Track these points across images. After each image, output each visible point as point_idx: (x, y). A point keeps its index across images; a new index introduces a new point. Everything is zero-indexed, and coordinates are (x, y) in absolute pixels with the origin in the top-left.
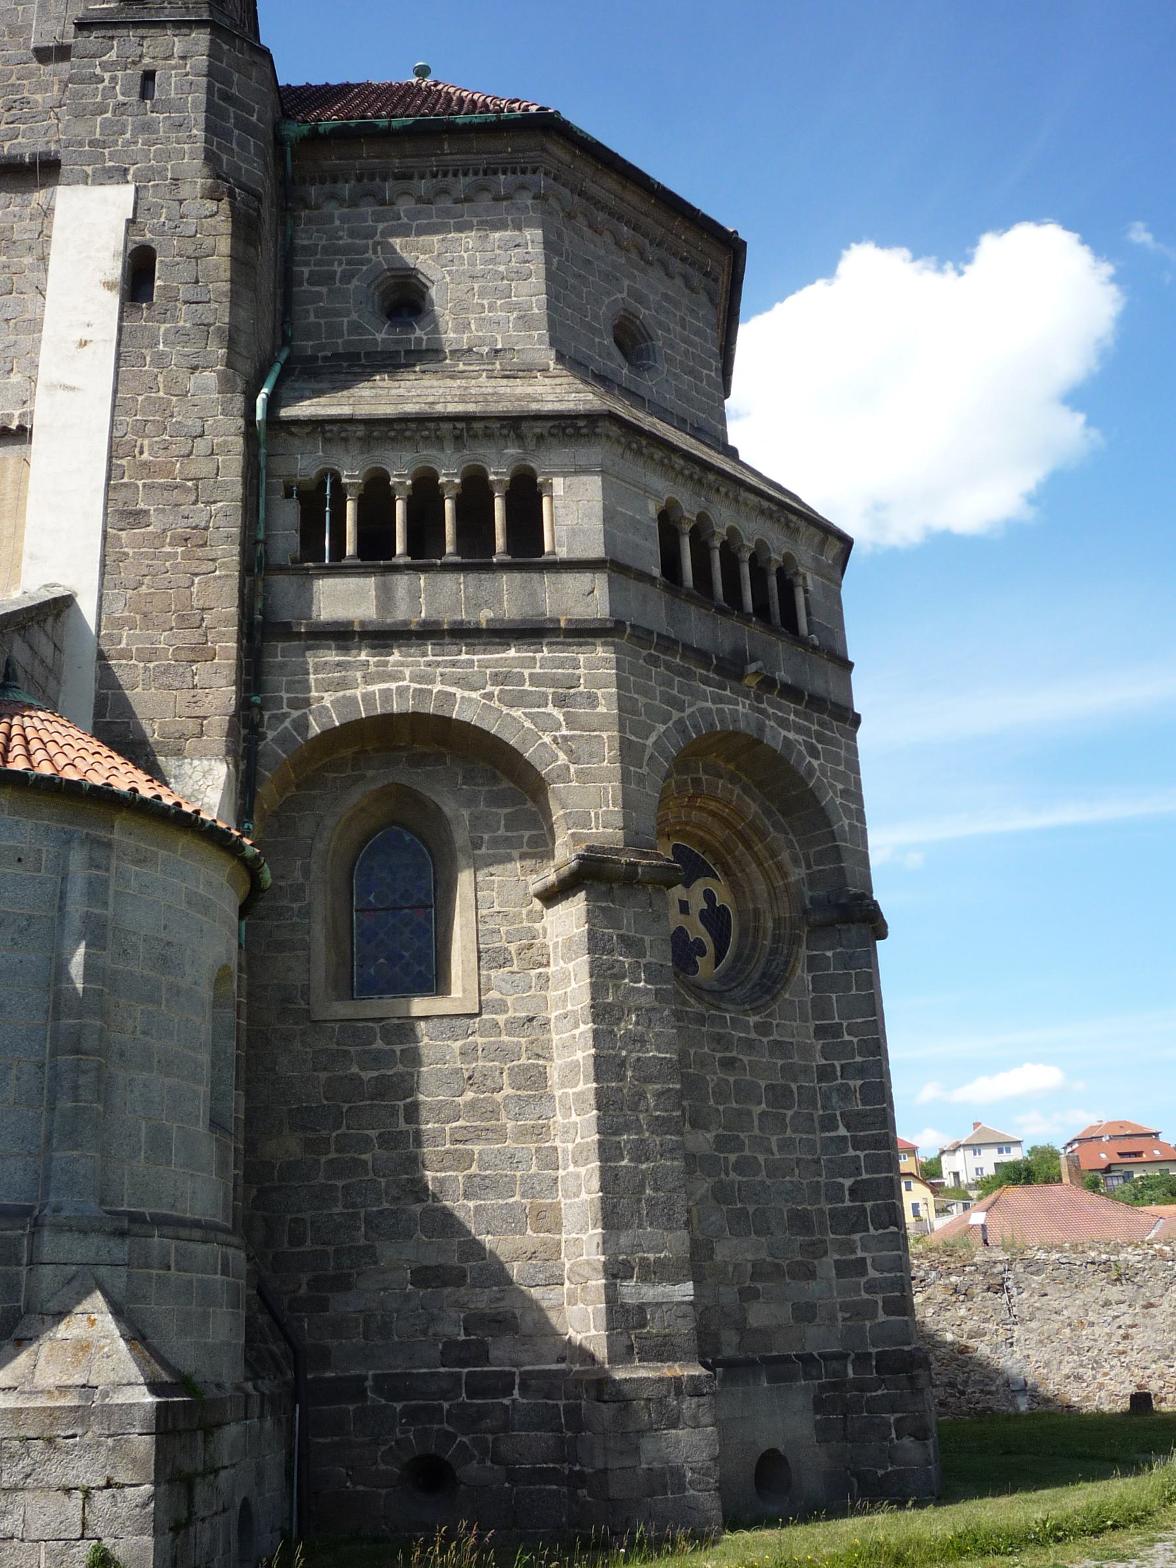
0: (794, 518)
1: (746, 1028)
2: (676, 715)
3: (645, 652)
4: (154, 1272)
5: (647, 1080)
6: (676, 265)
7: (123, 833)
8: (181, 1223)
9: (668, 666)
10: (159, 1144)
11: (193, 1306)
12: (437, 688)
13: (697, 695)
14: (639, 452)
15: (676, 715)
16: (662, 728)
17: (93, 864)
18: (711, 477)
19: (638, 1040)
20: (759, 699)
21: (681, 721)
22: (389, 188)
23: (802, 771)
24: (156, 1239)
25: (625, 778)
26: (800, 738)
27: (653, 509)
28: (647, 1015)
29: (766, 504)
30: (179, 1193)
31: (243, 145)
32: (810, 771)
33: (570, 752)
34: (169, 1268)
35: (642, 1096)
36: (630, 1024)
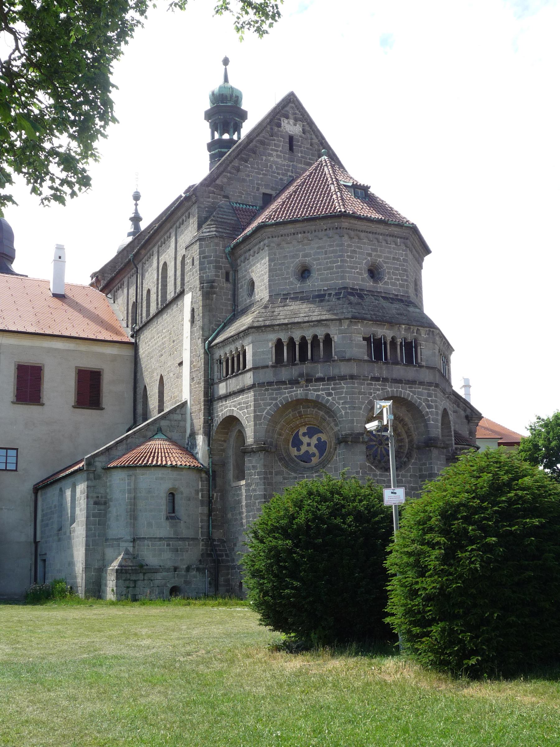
0: (325, 322)
1: (313, 477)
2: (274, 402)
3: (264, 389)
5: (257, 499)
6: (321, 234)
7: (138, 471)
8: (155, 538)
9: (272, 389)
10: (150, 525)
12: (232, 408)
13: (281, 394)
14: (262, 331)
15: (274, 402)
16: (269, 408)
17: (128, 479)
18: (289, 326)
19: (254, 490)
20: (307, 386)
21: (276, 403)
22: (247, 254)
23: (324, 402)
25: (255, 425)
26: (324, 392)
27: (270, 344)
28: (257, 484)
29: (312, 324)
31: (209, 269)
32: (328, 400)
33: (247, 421)
35: (255, 503)
36: (253, 487)
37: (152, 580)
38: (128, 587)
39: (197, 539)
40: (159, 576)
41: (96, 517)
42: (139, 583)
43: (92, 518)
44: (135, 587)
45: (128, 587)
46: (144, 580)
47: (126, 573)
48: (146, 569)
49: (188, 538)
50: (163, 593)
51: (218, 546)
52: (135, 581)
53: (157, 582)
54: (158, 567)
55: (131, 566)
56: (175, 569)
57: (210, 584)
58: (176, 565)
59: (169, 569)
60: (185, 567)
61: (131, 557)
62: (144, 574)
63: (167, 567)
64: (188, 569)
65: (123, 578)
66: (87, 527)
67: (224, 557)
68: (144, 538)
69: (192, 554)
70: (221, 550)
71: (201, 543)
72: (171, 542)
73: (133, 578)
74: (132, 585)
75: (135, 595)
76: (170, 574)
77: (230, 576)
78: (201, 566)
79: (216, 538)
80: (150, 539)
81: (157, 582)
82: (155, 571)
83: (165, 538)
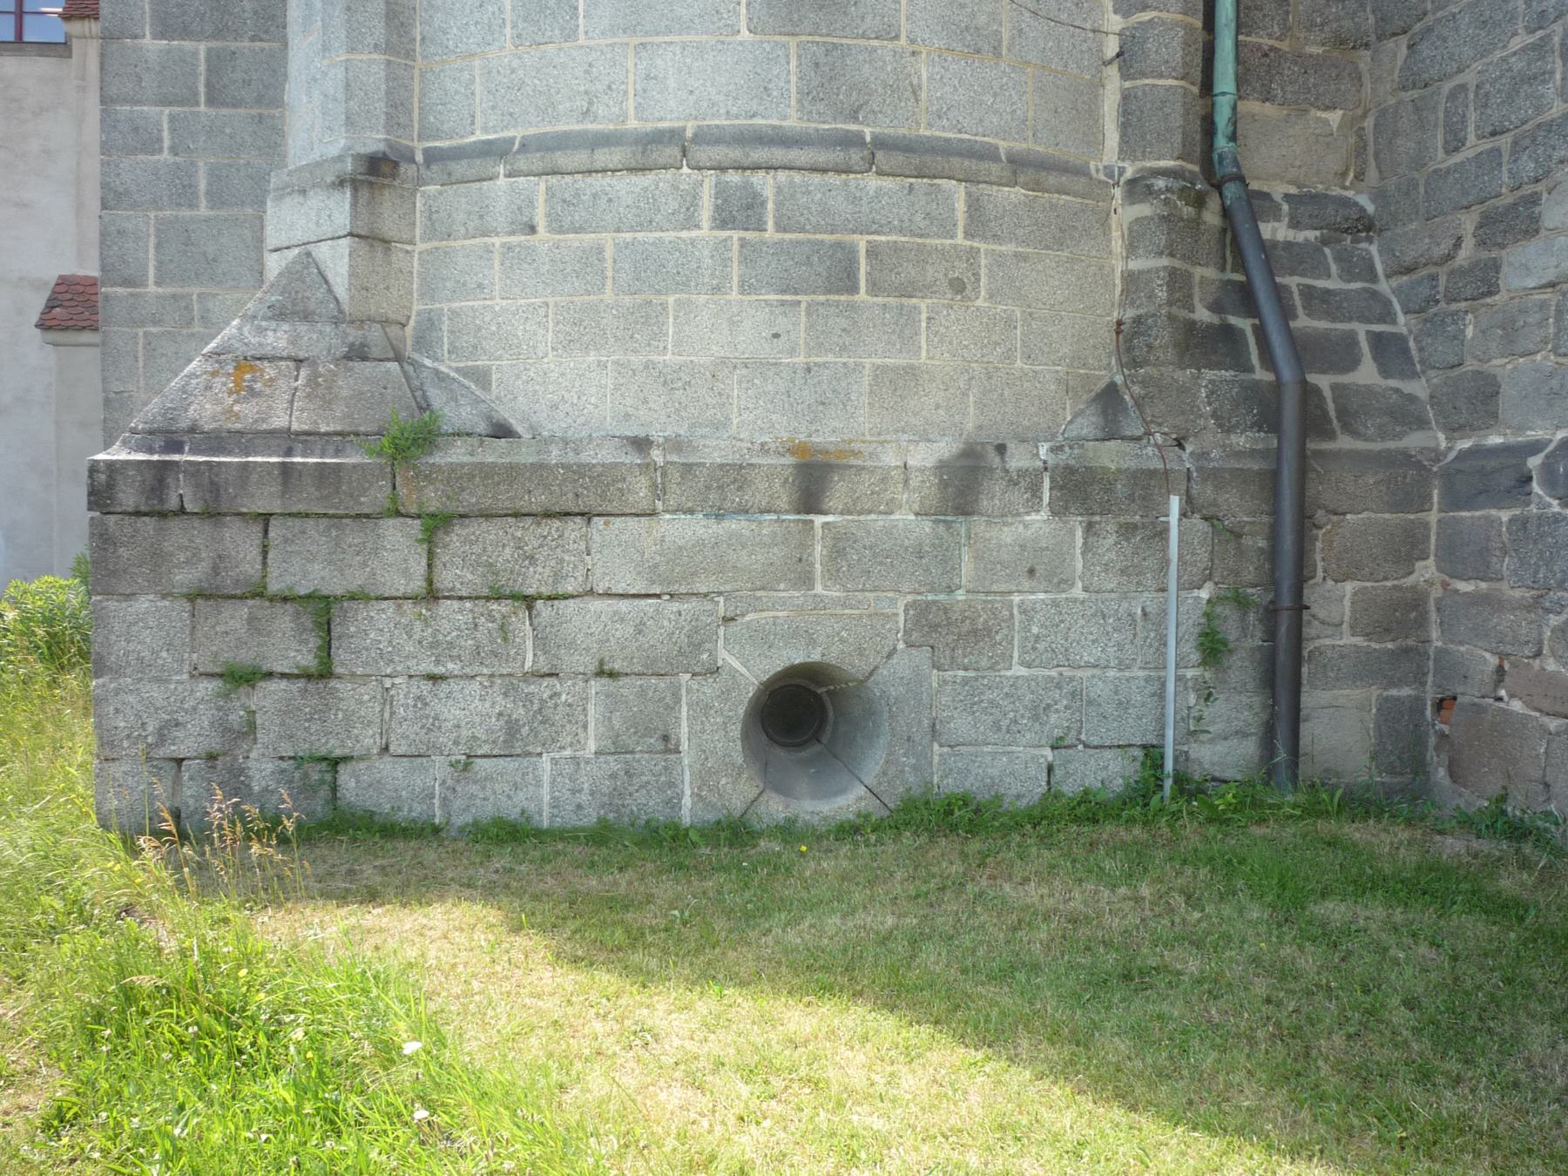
4: (497, 241)
11: (608, 296)
24: (502, 182)
30: (600, 87)
34: (532, 229)
37: (529, 601)
38: (242, 678)
39: (1081, 171)
40: (615, 551)
41: (186, 33)
42: (374, 632)
43: (151, 45)
44: (323, 673)
45: (242, 678)
46: (432, 595)
47: (212, 515)
48: (456, 477)
49: (989, 154)
50: (668, 743)
51: (1301, 258)
52: (323, 613)
53: (588, 623)
54: (606, 455)
55: (288, 440)
56: (812, 481)
57: (1212, 648)
58: (826, 434)
59: (736, 474)
60: (924, 456)
61: (320, 340)
62: (436, 525)
63: (715, 451)
64: (964, 484)
65: (185, 578)
66: (108, 122)
67: (1367, 373)
68: (494, 151)
69: (1014, 329)
70: (1318, 300)
71: (1125, 214)
72: (767, 184)
73: (306, 565)
74: (289, 648)
75: (335, 763)
76: (754, 537)
77: (1426, 571)
78: (1111, 456)
79: (1278, 190)
80: (546, 153)
81: (588, 623)
82: (575, 497)
83: (702, 137)
